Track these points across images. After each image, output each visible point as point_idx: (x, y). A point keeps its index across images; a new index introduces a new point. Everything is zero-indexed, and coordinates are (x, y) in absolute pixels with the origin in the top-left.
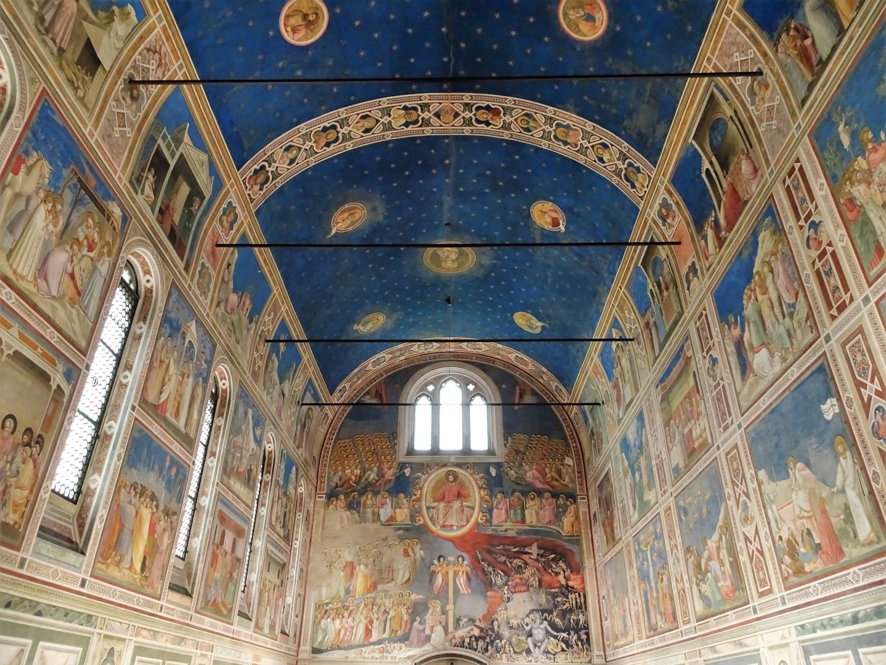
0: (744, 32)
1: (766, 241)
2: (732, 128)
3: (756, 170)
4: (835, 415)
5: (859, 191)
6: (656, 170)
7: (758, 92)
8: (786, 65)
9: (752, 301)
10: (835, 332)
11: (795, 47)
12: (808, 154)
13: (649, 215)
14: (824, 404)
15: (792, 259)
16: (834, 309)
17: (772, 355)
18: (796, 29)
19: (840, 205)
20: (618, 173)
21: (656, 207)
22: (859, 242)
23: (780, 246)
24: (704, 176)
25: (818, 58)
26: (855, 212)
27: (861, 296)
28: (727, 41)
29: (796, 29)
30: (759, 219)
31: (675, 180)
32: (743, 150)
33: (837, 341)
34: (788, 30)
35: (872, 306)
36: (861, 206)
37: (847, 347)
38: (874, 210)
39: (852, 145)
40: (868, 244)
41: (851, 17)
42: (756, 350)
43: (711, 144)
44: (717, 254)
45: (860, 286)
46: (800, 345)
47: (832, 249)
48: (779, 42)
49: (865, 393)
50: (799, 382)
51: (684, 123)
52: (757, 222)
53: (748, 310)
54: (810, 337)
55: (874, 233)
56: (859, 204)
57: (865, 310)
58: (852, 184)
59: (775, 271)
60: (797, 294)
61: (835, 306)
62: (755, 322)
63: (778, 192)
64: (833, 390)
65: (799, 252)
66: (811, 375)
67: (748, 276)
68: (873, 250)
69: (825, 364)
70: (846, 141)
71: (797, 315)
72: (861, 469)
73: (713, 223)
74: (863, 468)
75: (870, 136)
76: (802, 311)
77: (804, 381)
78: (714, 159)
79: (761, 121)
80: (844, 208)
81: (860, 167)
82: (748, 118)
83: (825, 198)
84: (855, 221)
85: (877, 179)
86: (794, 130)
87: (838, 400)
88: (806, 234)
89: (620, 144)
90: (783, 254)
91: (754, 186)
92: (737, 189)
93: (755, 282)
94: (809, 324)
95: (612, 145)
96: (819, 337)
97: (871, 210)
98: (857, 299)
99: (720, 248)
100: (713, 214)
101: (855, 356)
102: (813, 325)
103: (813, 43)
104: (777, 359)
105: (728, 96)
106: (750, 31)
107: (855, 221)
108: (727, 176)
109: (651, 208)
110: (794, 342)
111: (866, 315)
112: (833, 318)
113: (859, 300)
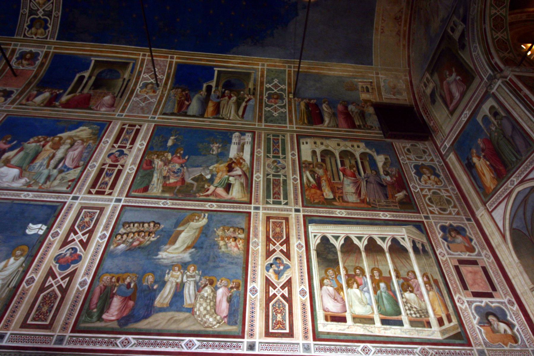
0: (168, 69)
1: (84, 132)
2: (120, 82)
3: (112, 106)
4: (36, 234)
5: (158, 163)
6: (55, 41)
7: (148, 88)
8: (170, 97)
9: (38, 144)
10: (83, 198)
11: (180, 98)
12: (148, 129)
13: (16, 45)
14: (34, 224)
15: (92, 152)
16: (95, 190)
17: (21, 176)
18: (187, 94)
19: (144, 159)
20: (32, 12)
21: (28, 49)
22: (139, 178)
23: (91, 142)
24: (78, 76)
25: (185, 111)
26: (148, 167)
27: (117, 196)
28: (159, 62)
29: (187, 94)
30: (91, 121)
31: (56, 56)
32: (115, 93)
33: (81, 203)
34: (183, 91)
35: (119, 205)
36: (154, 168)
37: (84, 210)
38: (158, 175)
39: (171, 147)
40: (143, 182)
41: (209, 116)
42: (8, 165)
43: (101, 73)
44: (39, 105)
45: (120, 193)
46: (50, 187)
47: (121, 168)
48: (176, 89)
49: (72, 235)
50: (27, 202)
51: (101, 52)
52: (88, 121)
53: (29, 145)
54: (64, 189)
55: (150, 181)
56: (153, 166)
57: (113, 203)
58: (157, 158)
59: (74, 147)
60: (76, 167)
61: (96, 189)
62: (27, 154)
63: (116, 124)
64: (50, 222)
65: (100, 154)
66: (42, 206)
67: (53, 133)
68: (142, 187)
69: (60, 208)
70: (170, 143)
71: (66, 174)
72: (23, 271)
73: (54, 94)
74: (25, 272)
75: (182, 152)
76: (73, 174)
77: (32, 205)
78: (93, 78)
79: (137, 96)
80: (144, 161)
81: (167, 156)
82: (132, 89)
83: (139, 150)
84: (145, 170)
85: (170, 167)
86: (150, 116)
87: (47, 229)
88: (114, 151)
89: (57, 9)
90: (89, 145)
91: (103, 109)
92: (91, 100)
93: (53, 139)
94: (70, 183)
95: (52, 3)
96: (71, 193)
97: (157, 174)
98: (114, 196)
99: (46, 106)
100: (61, 91)
101: (85, 217)
102: (72, 186)
103: (189, 105)
104: (23, 181)
105: (134, 72)
106: (171, 72)
107: (145, 170)
108: (91, 90)
109: (21, 45)
110: (48, 183)
111: (112, 206)
112: (90, 193)
113: (115, 197)
